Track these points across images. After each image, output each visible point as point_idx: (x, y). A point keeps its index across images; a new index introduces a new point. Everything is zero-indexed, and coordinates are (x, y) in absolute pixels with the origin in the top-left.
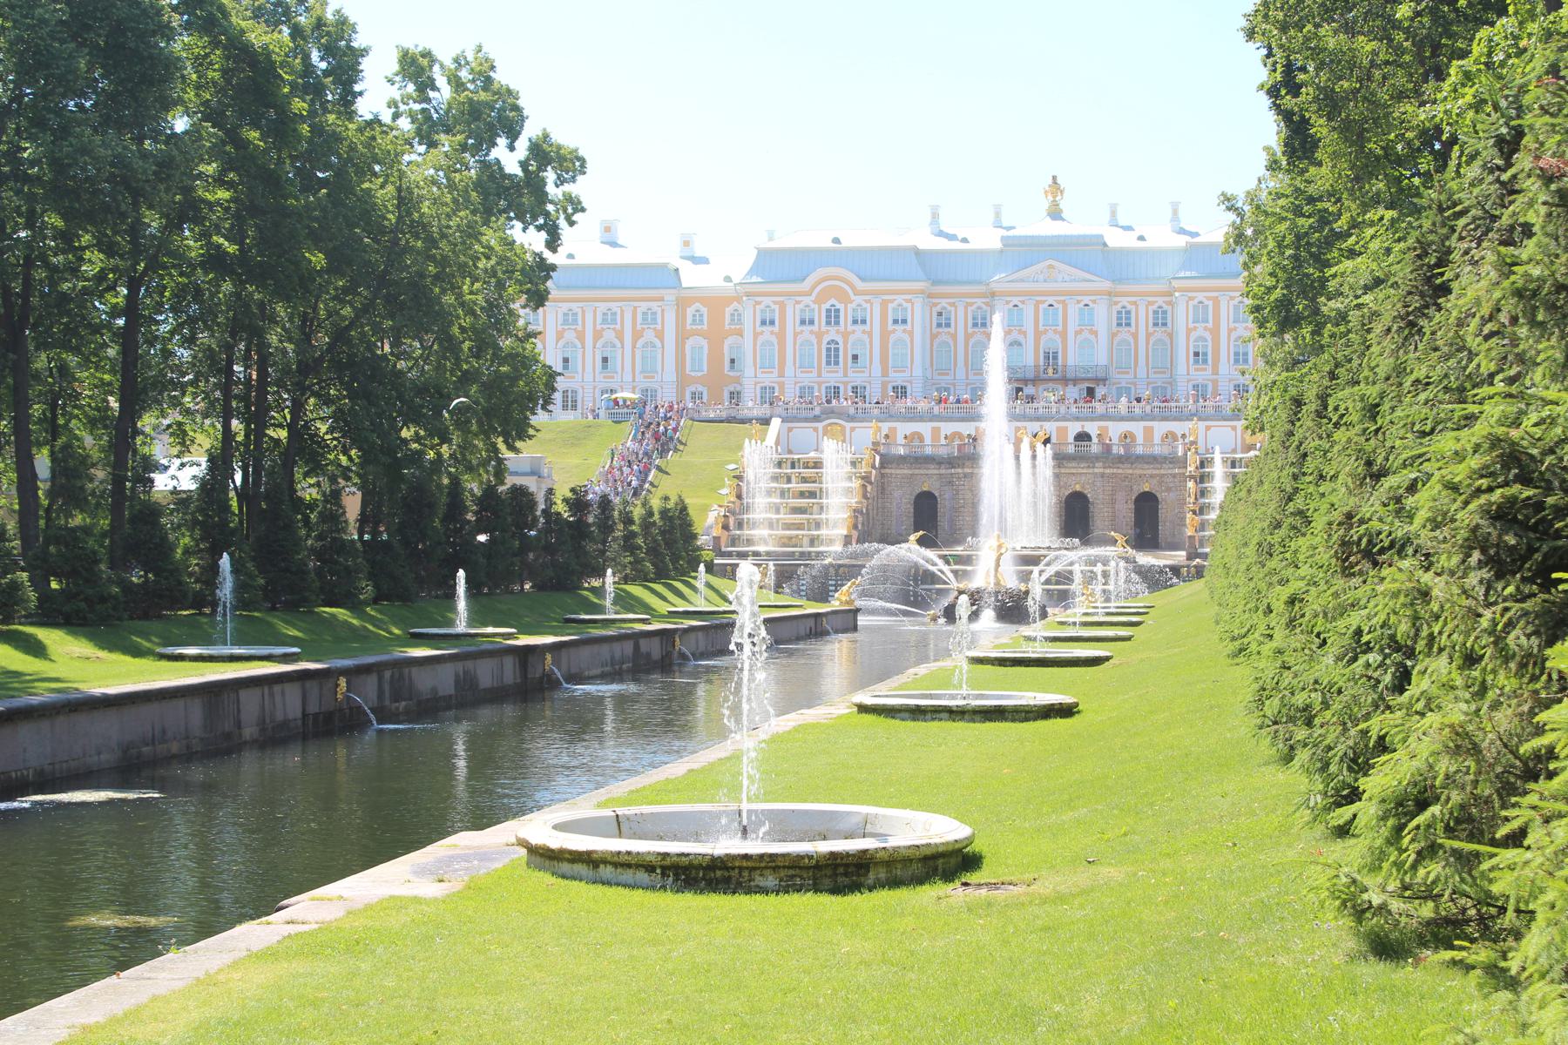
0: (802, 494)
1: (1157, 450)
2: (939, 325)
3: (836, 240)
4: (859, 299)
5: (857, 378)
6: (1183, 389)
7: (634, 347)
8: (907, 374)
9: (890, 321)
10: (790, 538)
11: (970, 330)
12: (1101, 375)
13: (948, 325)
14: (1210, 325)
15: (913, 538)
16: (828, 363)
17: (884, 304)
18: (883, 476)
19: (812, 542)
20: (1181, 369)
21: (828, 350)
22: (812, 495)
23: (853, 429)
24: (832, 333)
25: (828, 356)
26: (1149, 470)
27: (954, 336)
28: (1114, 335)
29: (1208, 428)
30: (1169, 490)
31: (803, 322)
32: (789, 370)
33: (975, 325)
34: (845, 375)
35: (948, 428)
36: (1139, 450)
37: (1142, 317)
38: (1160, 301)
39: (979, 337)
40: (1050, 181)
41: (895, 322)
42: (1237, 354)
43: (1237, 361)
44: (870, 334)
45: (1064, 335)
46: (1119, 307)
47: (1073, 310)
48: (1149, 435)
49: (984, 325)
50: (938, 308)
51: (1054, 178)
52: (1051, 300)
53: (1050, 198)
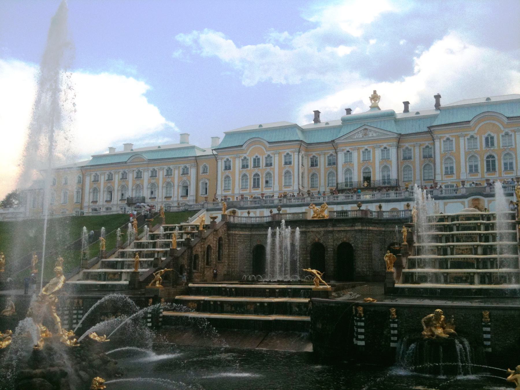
2: (312, 165)
7: (179, 186)
8: (291, 189)
9: (283, 163)
10: (115, 274)
11: (327, 167)
12: (393, 183)
13: (317, 165)
14: (454, 151)
16: (254, 187)
18: (229, 235)
21: (254, 179)
24: (256, 170)
25: (254, 183)
27: (320, 169)
29: (445, 204)
32: (237, 191)
33: (329, 164)
34: (262, 190)
40: (372, 93)
41: (286, 163)
42: (471, 167)
43: (471, 171)
46: (404, 148)
47: (378, 153)
50: (311, 156)
51: (375, 92)
52: (366, 147)
53: (373, 102)
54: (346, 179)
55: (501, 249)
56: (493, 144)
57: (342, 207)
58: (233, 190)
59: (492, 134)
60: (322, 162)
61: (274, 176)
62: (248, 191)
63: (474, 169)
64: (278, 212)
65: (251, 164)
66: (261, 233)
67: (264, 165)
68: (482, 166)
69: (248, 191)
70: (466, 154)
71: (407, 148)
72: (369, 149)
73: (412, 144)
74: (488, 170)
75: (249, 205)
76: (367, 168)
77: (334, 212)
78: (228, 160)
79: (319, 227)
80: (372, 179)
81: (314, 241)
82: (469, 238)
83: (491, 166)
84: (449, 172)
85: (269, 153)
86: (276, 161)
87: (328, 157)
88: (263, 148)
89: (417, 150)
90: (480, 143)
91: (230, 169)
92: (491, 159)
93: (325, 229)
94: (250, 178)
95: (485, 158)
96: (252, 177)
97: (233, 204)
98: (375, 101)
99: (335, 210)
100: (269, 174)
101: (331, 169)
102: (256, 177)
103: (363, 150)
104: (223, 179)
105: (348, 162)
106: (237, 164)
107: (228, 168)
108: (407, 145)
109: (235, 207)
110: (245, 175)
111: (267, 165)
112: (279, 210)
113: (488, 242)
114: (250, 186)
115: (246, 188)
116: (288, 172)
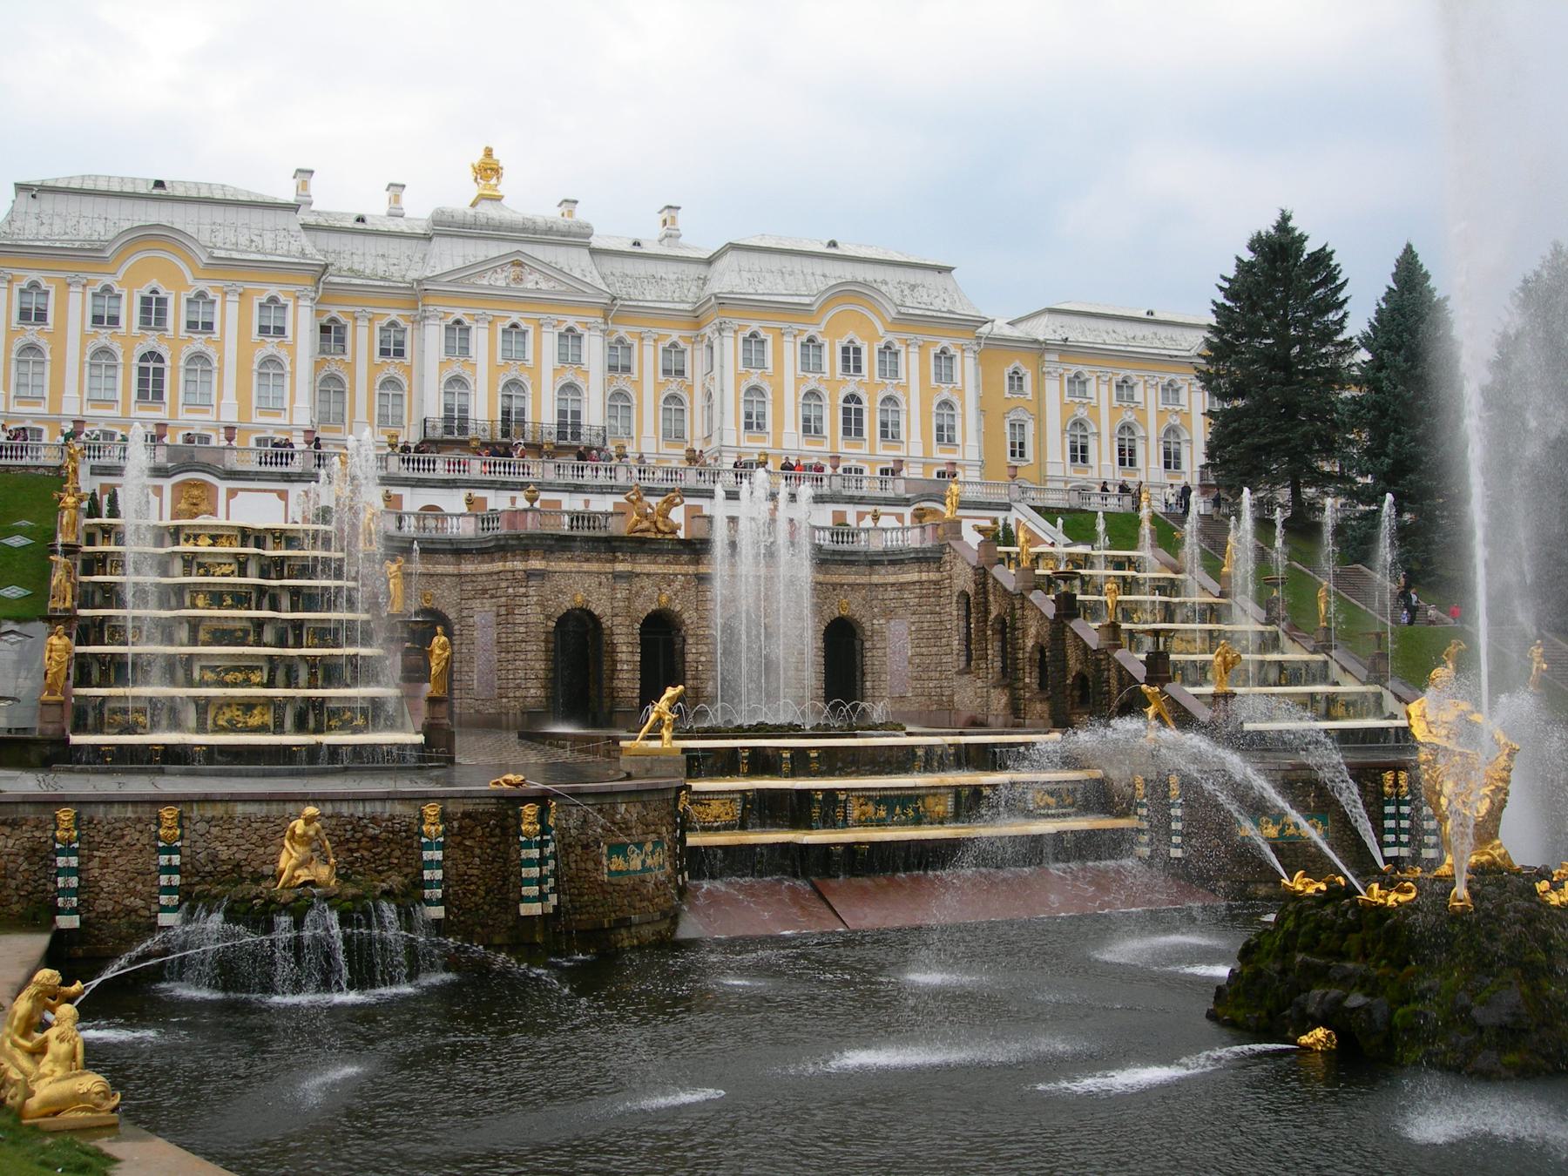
0: (216, 598)
3: (159, 184)
5: (198, 422)
8: (283, 420)
9: (256, 329)
10: (248, 705)
11: (378, 359)
15: (663, 704)
16: (142, 394)
19: (310, 715)
21: (143, 371)
23: (232, 493)
24: (151, 341)
25: (143, 382)
27: (351, 367)
28: (610, 383)
30: (889, 613)
31: (97, 320)
33: (384, 352)
34: (173, 412)
37: (647, 360)
38: (675, 336)
39: (392, 371)
41: (264, 330)
42: (807, 420)
43: (806, 429)
44: (220, 344)
45: (536, 371)
47: (550, 341)
49: (400, 353)
50: (324, 320)
51: (489, 152)
52: (515, 318)
54: (448, 409)
55: (259, 634)
56: (858, 369)
57: (587, 502)
58: (57, 400)
59: (858, 343)
60: (362, 340)
61: (221, 369)
62: (116, 412)
63: (810, 427)
64: (527, 505)
65: (130, 313)
66: (440, 569)
67: (183, 325)
68: (831, 420)
69: (116, 412)
71: (620, 341)
72: (523, 326)
73: (639, 330)
74: (847, 432)
75: (869, 488)
76: (514, 383)
77: (568, 512)
78: (34, 285)
79: (668, 562)
80: (529, 417)
81: (654, 607)
85: (201, 286)
86: (229, 316)
87: (382, 329)
88: (183, 266)
89: (649, 352)
90: (831, 358)
91: (41, 316)
92: (853, 406)
93: (691, 569)
94: (127, 367)
95: (840, 401)
96: (136, 361)
97: (192, 457)
98: (487, 179)
99: (565, 507)
100: (199, 357)
101: (392, 368)
102: (151, 365)
103: (507, 324)
104: (800, 399)
106: (76, 308)
108: (622, 331)
109: (206, 468)
110: (104, 351)
111: (192, 325)
112: (532, 500)
113: (1172, 621)
114: (126, 393)
115: (110, 403)
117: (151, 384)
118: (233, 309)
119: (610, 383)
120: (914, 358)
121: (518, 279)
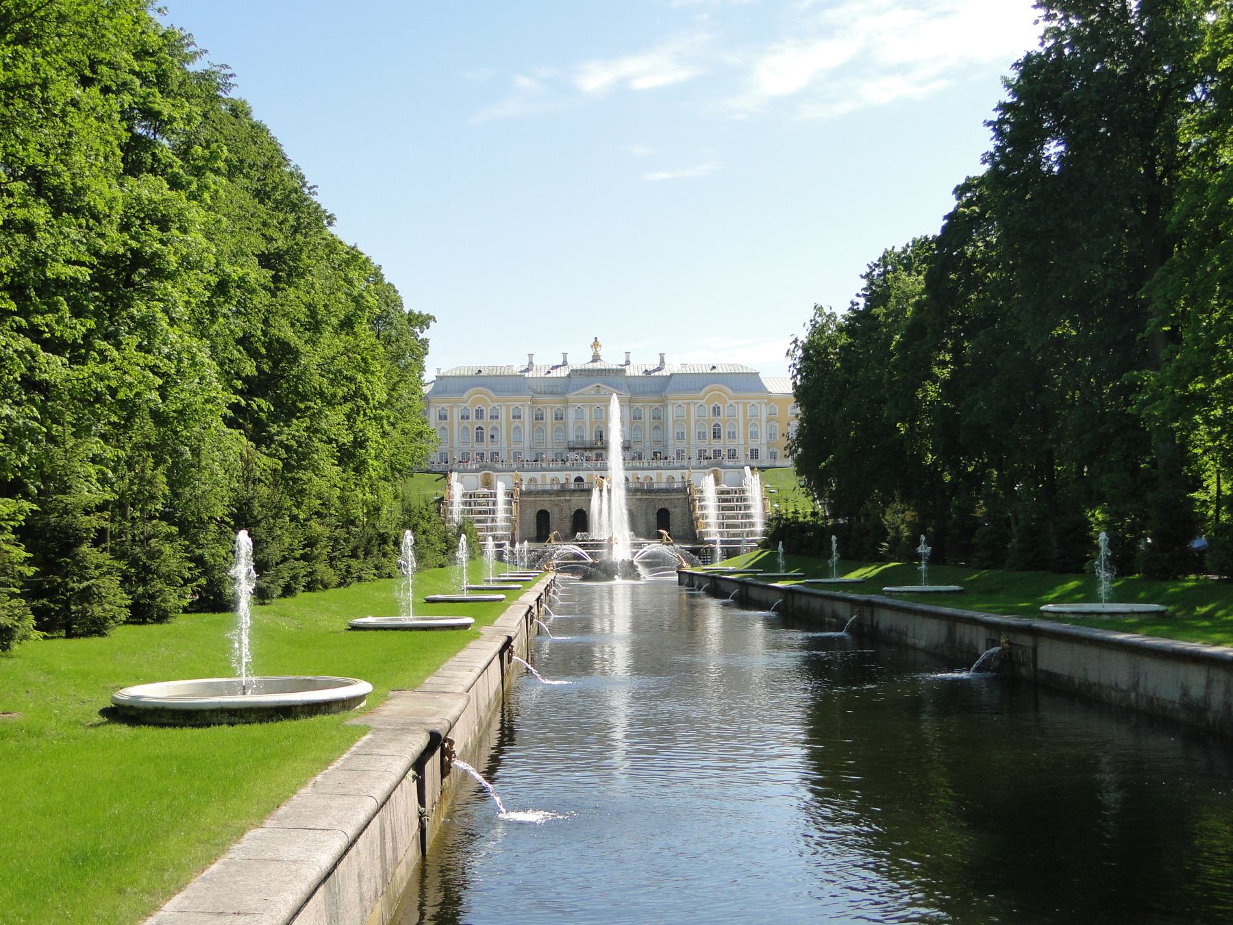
0: (480, 512)
1: (664, 486)
4: (495, 404)
6: (672, 453)
17: (508, 408)
20: (670, 442)
22: (485, 512)
26: (664, 496)
30: (675, 507)
31: (463, 418)
32: (456, 445)
35: (550, 475)
36: (655, 486)
37: (647, 414)
38: (657, 405)
41: (514, 417)
48: (660, 477)
60: (549, 416)
63: (701, 436)
65: (473, 416)
70: (697, 421)
82: (732, 509)
83: (716, 435)
84: (680, 436)
85: (495, 404)
86: (503, 413)
89: (647, 411)
91: (446, 418)
101: (559, 424)
105: (579, 418)
106: (457, 414)
107: (443, 417)
110: (466, 428)
111: (492, 417)
116: (517, 428)
117: (480, 438)
118: (504, 411)
119: (632, 424)
120: (741, 407)
121: (598, 392)
